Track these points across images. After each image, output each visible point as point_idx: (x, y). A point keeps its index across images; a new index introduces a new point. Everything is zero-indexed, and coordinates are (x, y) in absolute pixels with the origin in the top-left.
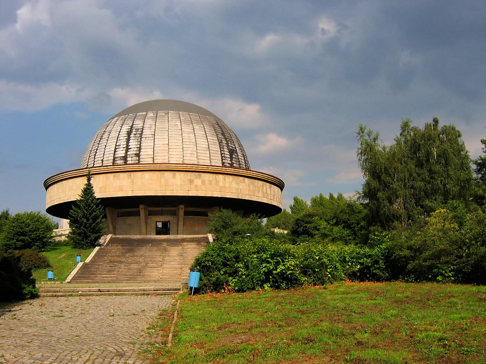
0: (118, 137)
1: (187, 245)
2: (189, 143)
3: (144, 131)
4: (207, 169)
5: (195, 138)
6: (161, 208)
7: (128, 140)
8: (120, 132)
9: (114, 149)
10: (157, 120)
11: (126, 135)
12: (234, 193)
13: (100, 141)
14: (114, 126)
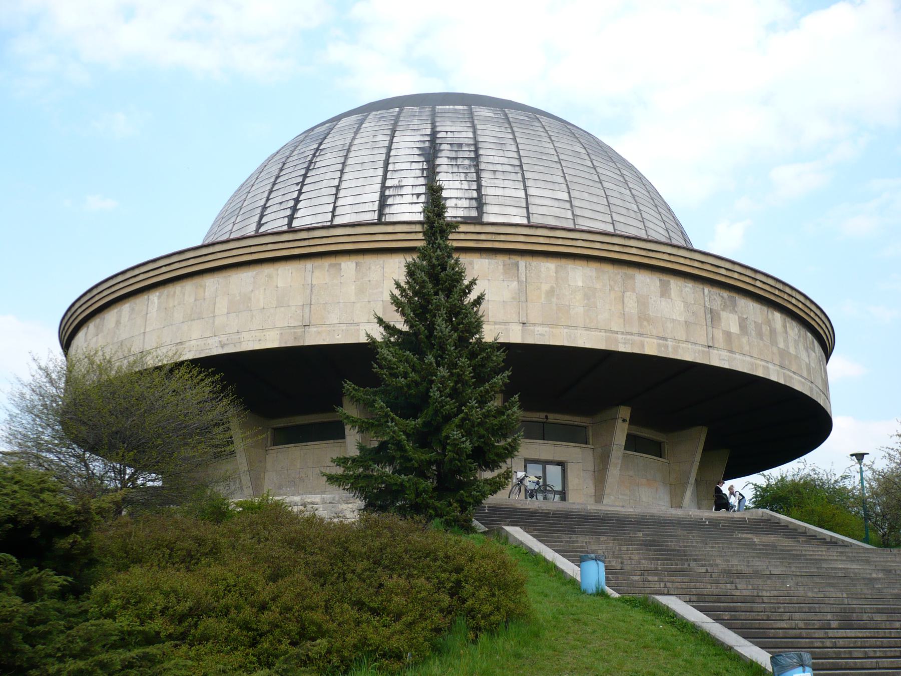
2: (624, 211)
6: (543, 415)
7: (431, 172)
8: (389, 149)
9: (376, 197)
11: (417, 158)
13: (305, 176)
14: (356, 133)
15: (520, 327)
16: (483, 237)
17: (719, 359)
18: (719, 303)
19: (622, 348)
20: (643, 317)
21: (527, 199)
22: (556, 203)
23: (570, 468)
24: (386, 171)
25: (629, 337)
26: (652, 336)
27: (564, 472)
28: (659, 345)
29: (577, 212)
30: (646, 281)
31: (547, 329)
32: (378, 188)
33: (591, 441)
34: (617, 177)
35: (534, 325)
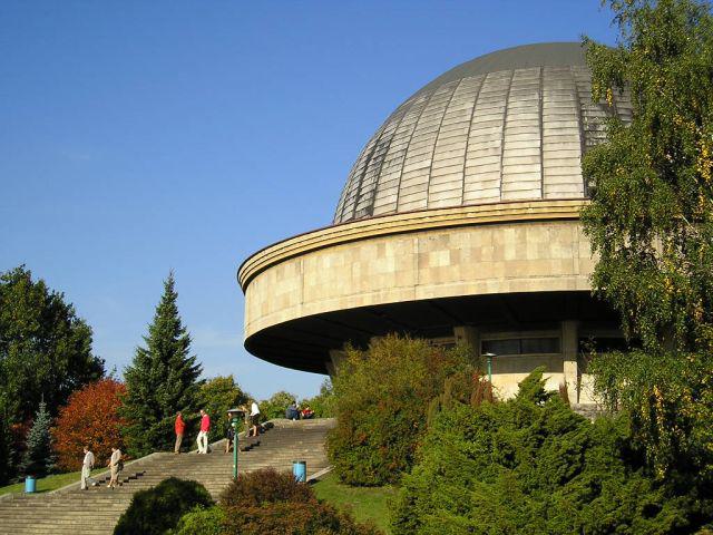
17: (422, 294)
28: (374, 297)
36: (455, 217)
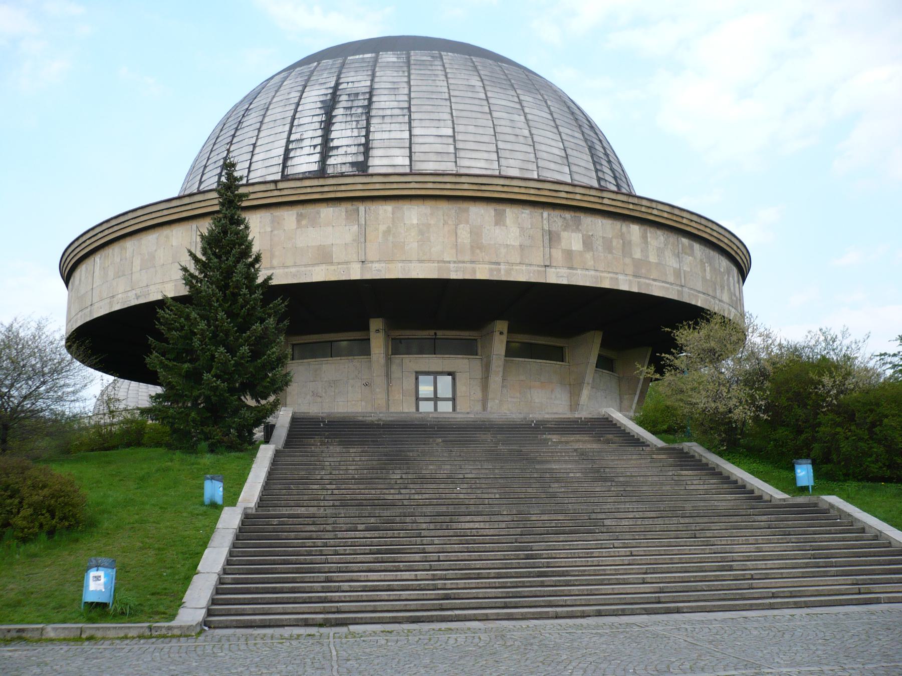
0: (293, 118)
1: (567, 442)
2: (512, 138)
3: (374, 99)
4: (600, 201)
5: (529, 127)
6: (432, 332)
7: (327, 126)
8: (298, 104)
9: (282, 151)
10: (412, 71)
11: (318, 112)
12: (672, 284)
13: (234, 136)
14: (277, 91)
15: (359, 265)
16: (326, 189)
17: (557, 276)
18: (560, 224)
19: (453, 276)
20: (477, 246)
21: (411, 139)
22: (439, 140)
23: (458, 375)
24: (292, 126)
25: (461, 265)
26: (484, 262)
27: (454, 379)
28: (491, 270)
29: (460, 145)
30: (480, 213)
31: (383, 265)
32: (284, 142)
33: (479, 351)
34: (512, 105)
35: (372, 262)
36: (592, 199)
